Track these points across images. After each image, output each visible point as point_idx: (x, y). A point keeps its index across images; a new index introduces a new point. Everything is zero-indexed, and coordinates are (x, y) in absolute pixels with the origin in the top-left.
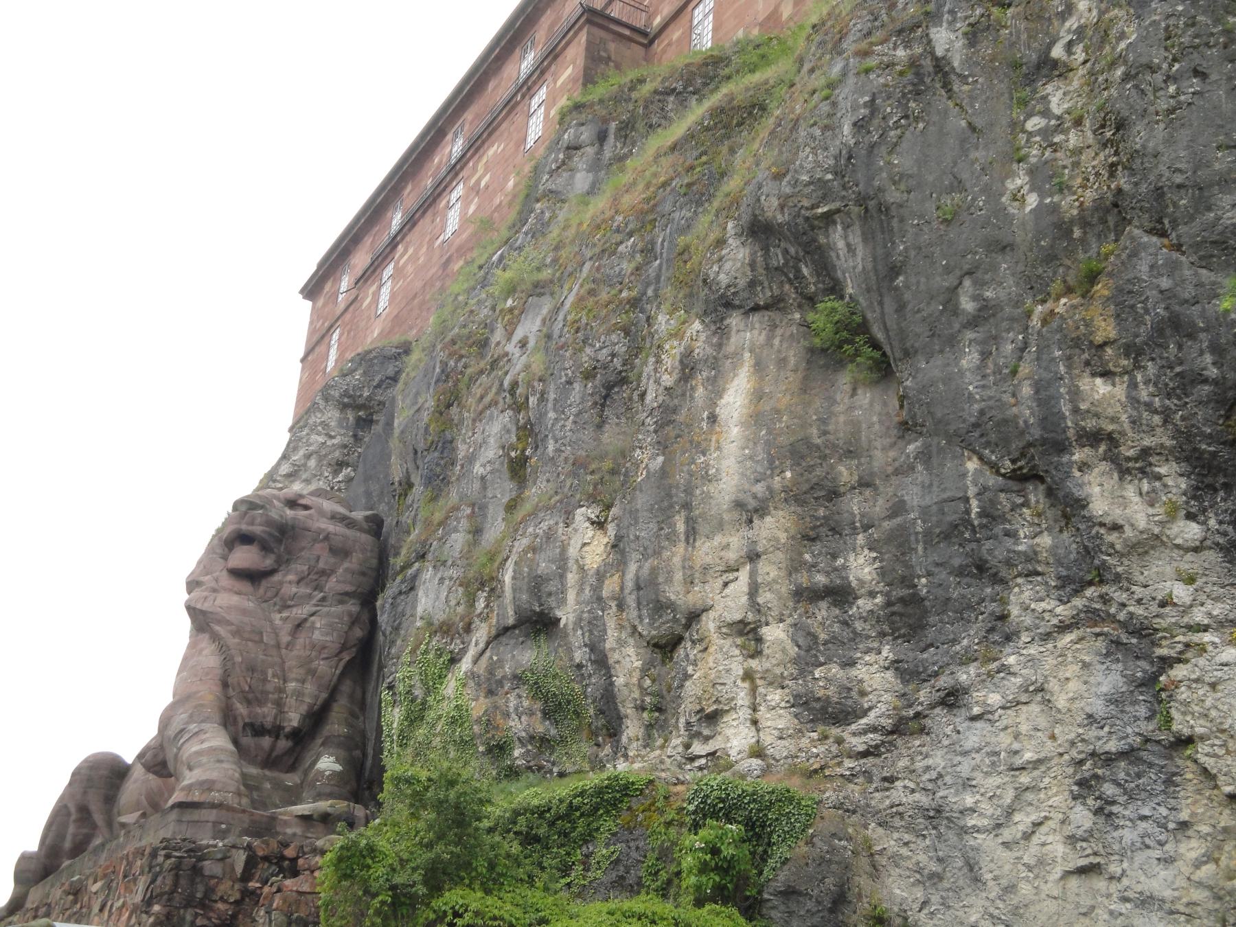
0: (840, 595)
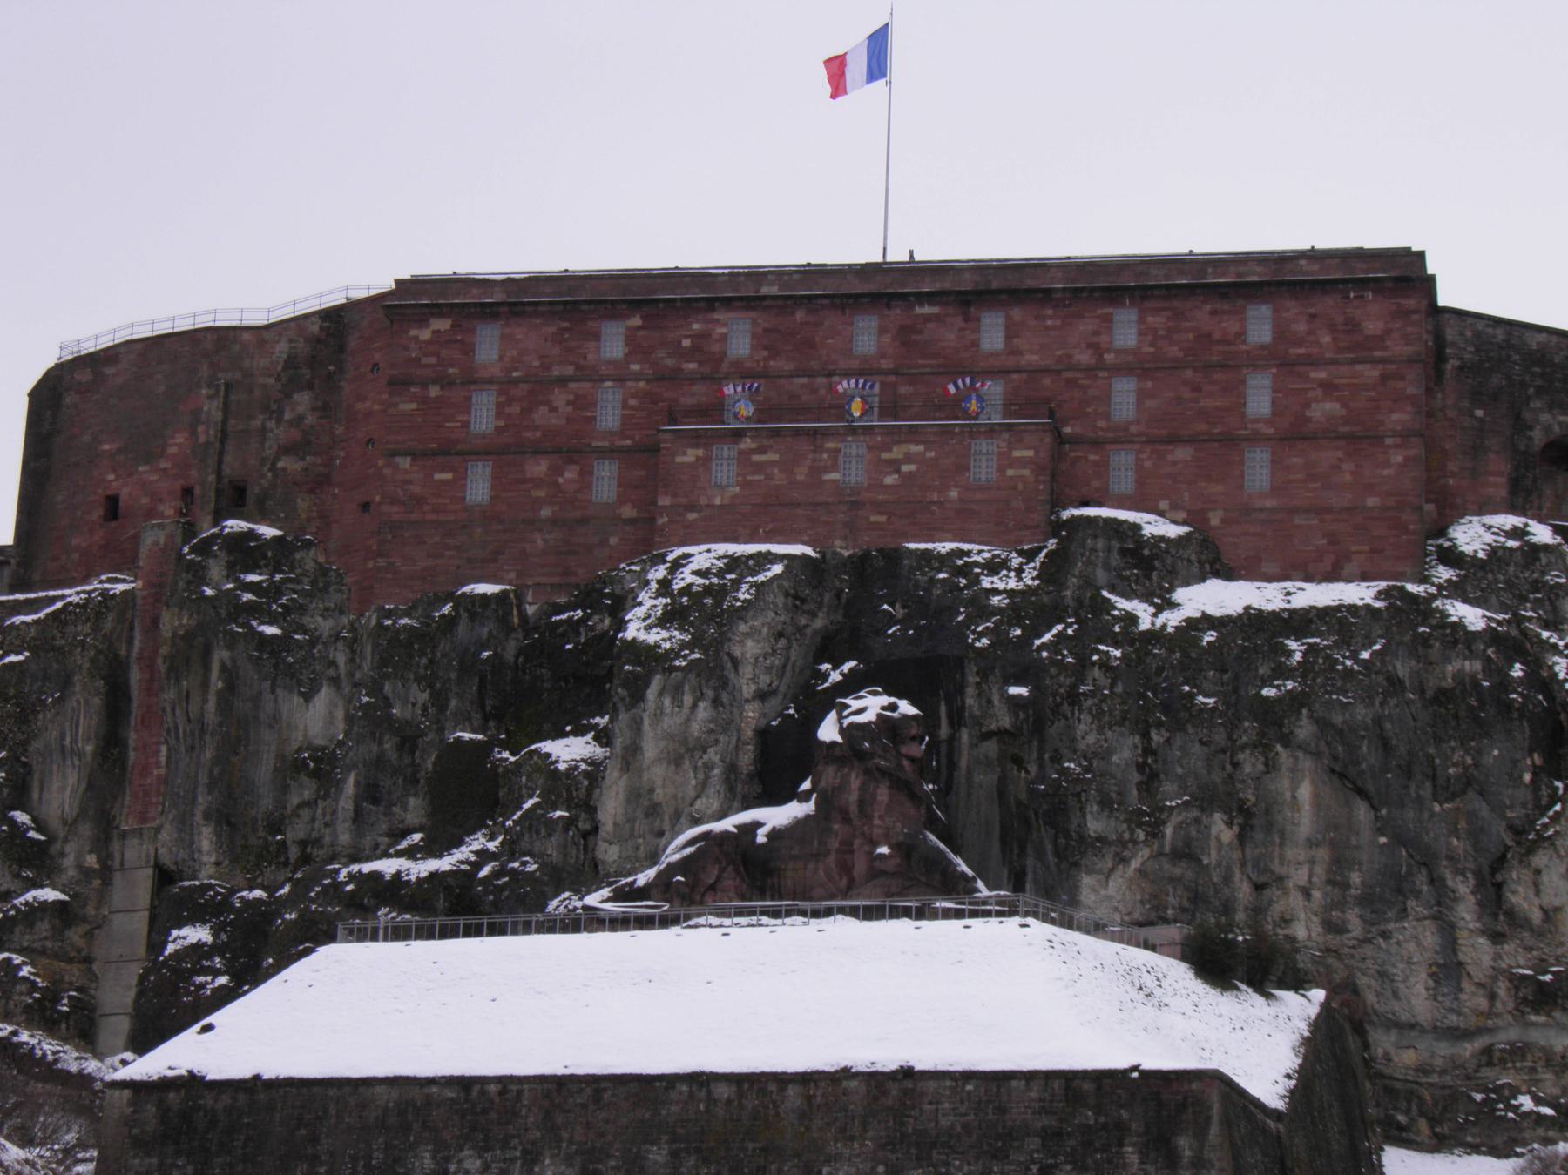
0: (1345, 886)
